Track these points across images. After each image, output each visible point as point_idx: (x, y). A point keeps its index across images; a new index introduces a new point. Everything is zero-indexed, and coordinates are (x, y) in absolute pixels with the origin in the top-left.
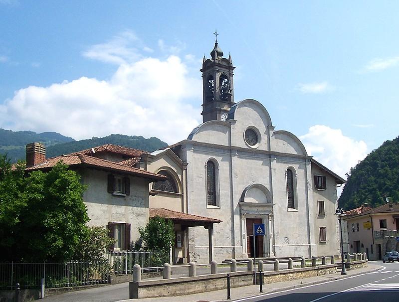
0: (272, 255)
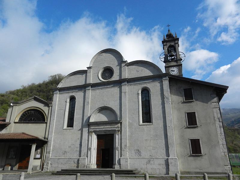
0: (117, 167)
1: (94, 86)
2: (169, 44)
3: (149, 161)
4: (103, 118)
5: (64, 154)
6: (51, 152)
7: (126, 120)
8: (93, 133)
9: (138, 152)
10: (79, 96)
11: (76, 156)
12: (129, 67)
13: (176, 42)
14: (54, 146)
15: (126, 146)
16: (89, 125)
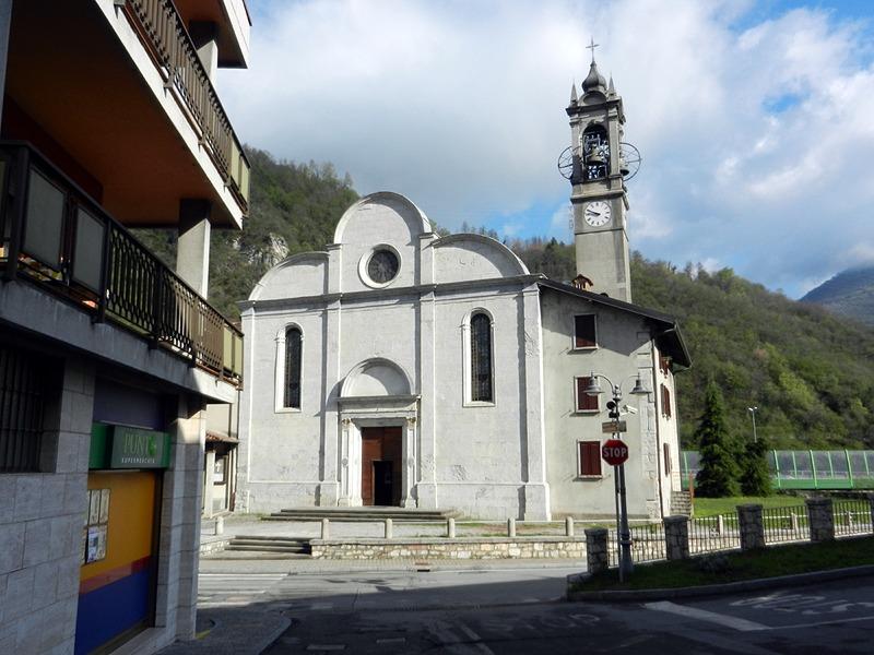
0: (409, 504)
1: (349, 299)
2: (590, 119)
3: (484, 491)
4: (375, 387)
5: (282, 473)
6: (249, 469)
7: (432, 394)
8: (351, 424)
9: (459, 469)
10: (309, 322)
11: (312, 479)
12: (442, 249)
13: (613, 112)
14: (255, 454)
15: (431, 456)
16: (339, 403)
